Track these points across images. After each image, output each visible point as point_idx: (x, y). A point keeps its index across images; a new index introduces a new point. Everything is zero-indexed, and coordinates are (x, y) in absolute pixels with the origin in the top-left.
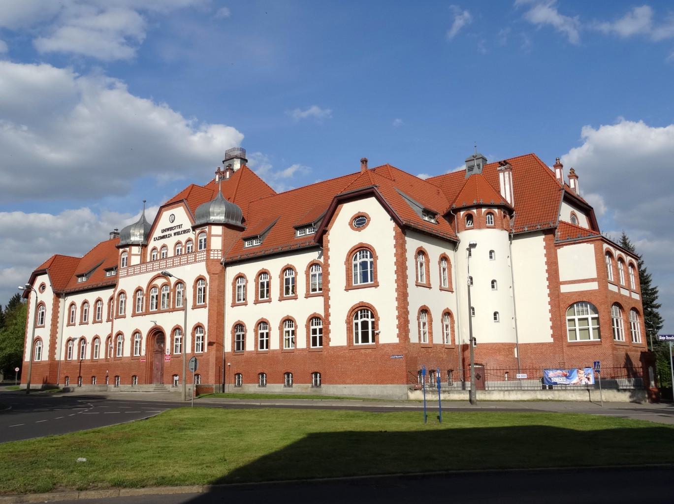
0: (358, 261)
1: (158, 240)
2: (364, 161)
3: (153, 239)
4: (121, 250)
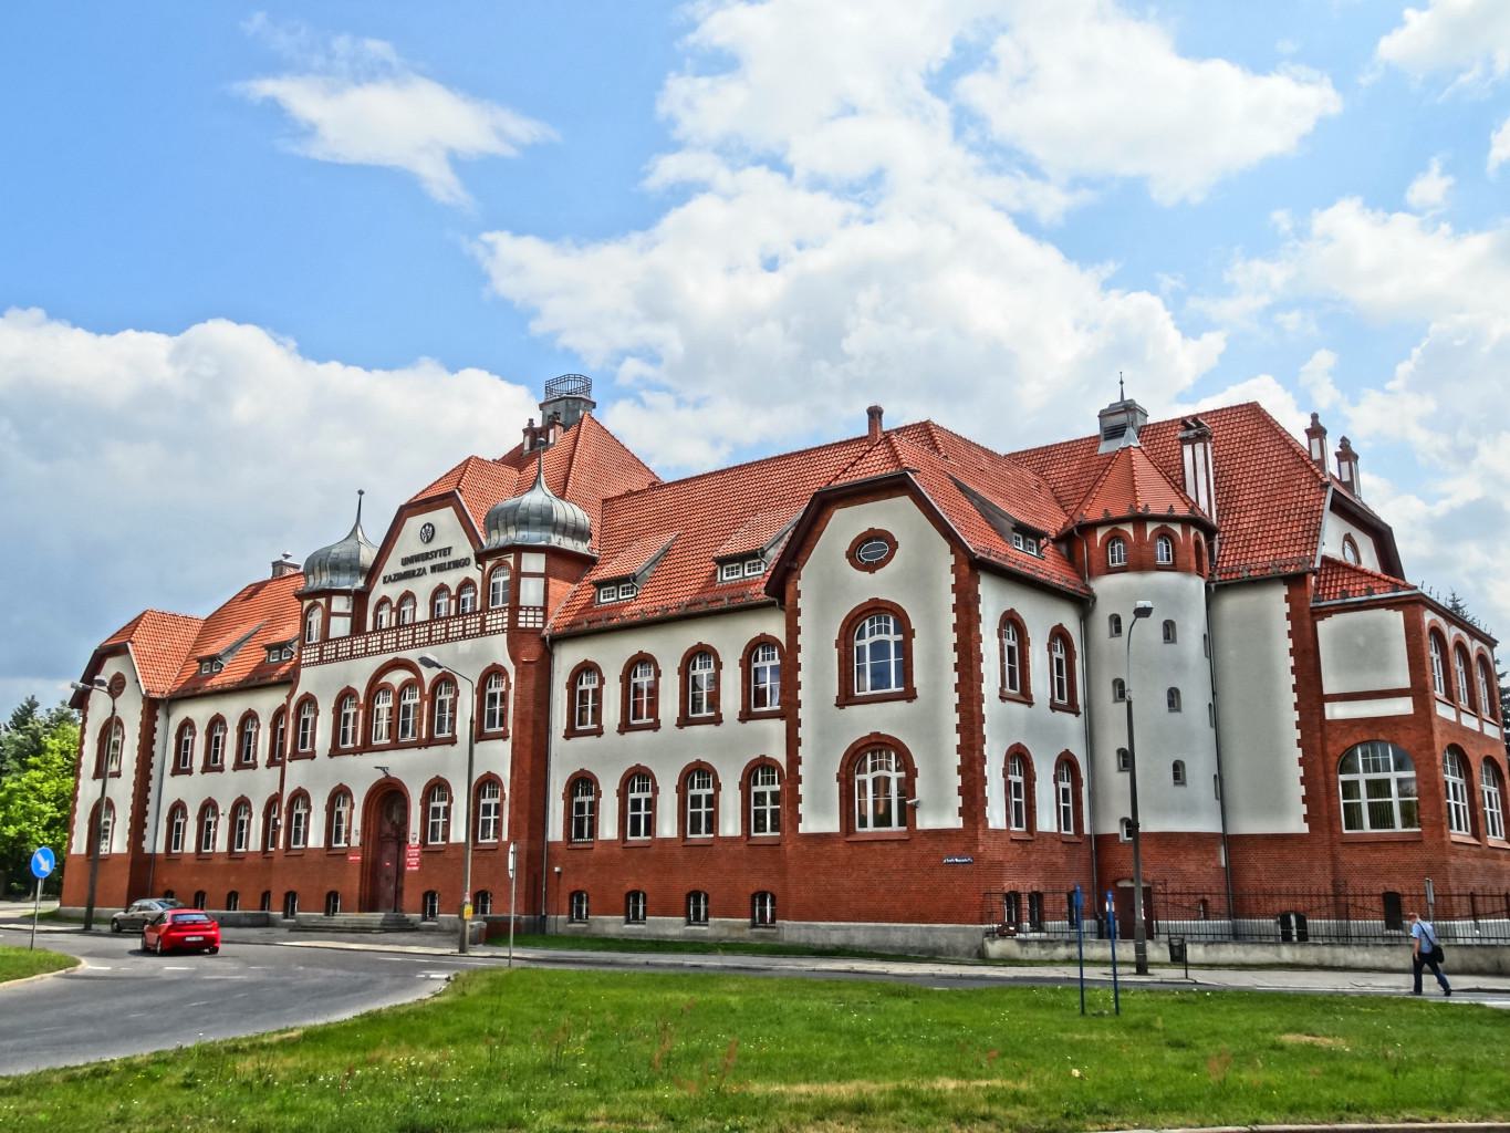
0: (867, 642)
1: (394, 580)
2: (875, 414)
3: (381, 579)
4: (307, 603)
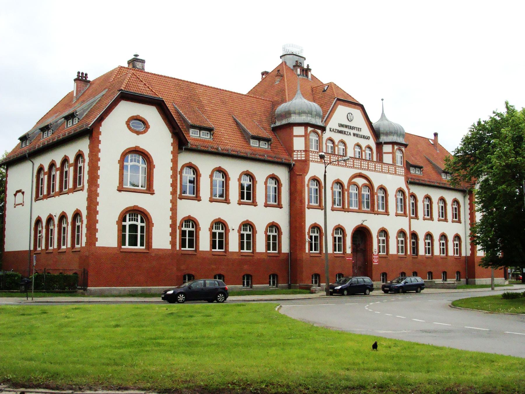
1: (335, 132)
